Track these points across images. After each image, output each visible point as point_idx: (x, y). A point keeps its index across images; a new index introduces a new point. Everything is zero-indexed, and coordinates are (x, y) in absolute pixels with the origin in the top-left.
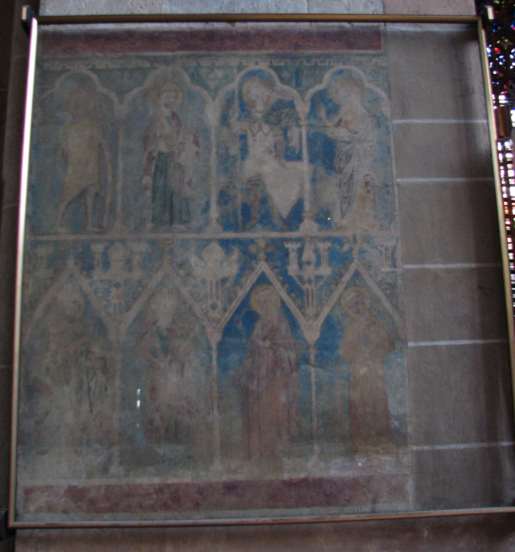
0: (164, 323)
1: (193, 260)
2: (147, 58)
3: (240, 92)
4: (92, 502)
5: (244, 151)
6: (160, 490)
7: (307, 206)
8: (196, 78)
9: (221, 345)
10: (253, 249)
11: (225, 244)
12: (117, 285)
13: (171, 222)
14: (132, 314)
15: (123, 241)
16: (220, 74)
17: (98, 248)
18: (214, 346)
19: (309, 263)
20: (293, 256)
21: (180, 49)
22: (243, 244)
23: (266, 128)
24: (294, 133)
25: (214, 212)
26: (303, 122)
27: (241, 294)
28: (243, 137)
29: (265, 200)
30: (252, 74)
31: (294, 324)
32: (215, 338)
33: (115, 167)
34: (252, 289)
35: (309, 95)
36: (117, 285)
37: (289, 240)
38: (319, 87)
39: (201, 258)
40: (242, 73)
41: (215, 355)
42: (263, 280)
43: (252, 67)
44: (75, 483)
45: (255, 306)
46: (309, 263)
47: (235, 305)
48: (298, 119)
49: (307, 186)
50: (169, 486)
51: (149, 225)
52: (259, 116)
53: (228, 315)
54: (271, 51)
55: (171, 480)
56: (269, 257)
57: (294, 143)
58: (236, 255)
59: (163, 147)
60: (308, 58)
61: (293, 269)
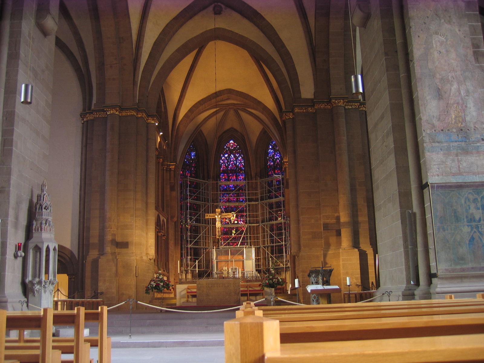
0: (458, 240)
1: (463, 229)
2: (450, 190)
3: (468, 197)
4: (450, 271)
5: (469, 208)
6: (461, 269)
7: (482, 218)
8: (459, 194)
9: (469, 243)
10: (473, 226)
11: (468, 226)
12: (450, 233)
13: (458, 222)
14: (453, 238)
15: (450, 225)
16: (464, 193)
17: (445, 227)
18: (468, 244)
19: (483, 229)
20: (480, 228)
21: (455, 188)
22: (471, 225)
23: (473, 204)
24: (478, 204)
25: (465, 220)
26: (480, 202)
27: (471, 234)
28: (469, 206)
29: (474, 217)
30: (469, 193)
31: (481, 240)
32: (467, 242)
33: (447, 211)
34: (473, 233)
35: (480, 197)
36: (450, 233)
37: (479, 224)
38: (482, 195)
39: (464, 228)
40: (468, 193)
41: (468, 245)
42: (475, 232)
43: (469, 192)
44: (446, 268)
45: (474, 236)
46: (483, 229)
47: (470, 237)
48: (479, 202)
49: (481, 214)
50: (462, 268)
51: (454, 222)
52: (471, 201)
53: (469, 238)
54: (473, 188)
55: (462, 267)
56: (476, 228)
57: (478, 206)
58: (470, 227)
59: (455, 208)
60: (480, 189)
61: (480, 230)
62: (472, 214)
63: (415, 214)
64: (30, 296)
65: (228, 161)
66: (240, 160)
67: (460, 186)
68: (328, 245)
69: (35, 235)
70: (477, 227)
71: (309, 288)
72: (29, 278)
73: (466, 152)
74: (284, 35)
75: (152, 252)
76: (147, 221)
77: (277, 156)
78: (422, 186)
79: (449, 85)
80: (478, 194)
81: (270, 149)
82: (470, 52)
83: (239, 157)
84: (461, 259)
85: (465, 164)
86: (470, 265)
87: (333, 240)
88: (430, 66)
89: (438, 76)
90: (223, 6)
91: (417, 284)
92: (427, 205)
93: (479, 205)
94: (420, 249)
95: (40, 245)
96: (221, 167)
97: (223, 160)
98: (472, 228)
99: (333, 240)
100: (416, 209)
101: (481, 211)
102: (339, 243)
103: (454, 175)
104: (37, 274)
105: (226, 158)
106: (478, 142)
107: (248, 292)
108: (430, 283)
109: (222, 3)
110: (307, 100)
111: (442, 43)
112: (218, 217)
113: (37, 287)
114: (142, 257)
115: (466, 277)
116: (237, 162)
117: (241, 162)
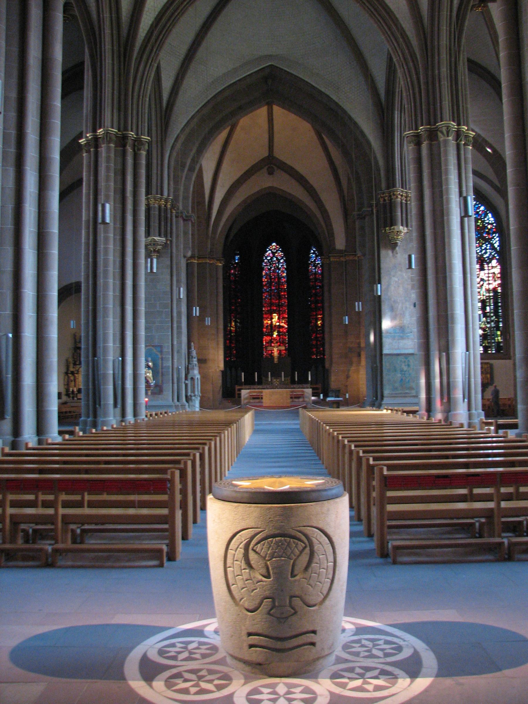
62: (403, 368)
63: (377, 366)
64: (190, 402)
65: (270, 264)
66: (281, 263)
67: (398, 355)
68: (351, 363)
69: (191, 372)
70: (404, 374)
71: (329, 399)
72: (189, 394)
73: (402, 338)
74: (324, 196)
75: (222, 366)
76: (218, 341)
77: (318, 261)
78: (381, 354)
79: (397, 305)
80: (406, 358)
81: (312, 253)
82: (410, 287)
83: (281, 259)
84: (396, 389)
85: (401, 345)
86: (400, 392)
87: (355, 359)
88: (389, 294)
89: (393, 300)
90: (275, 167)
91: (377, 399)
92: (384, 363)
93: (406, 364)
94: (379, 383)
95: (194, 377)
96: (263, 269)
97: (265, 263)
98: (402, 375)
99: (355, 359)
100: (378, 365)
101: (407, 367)
102: (359, 362)
103: (396, 349)
104: (193, 391)
105: (268, 260)
106: (409, 333)
107: (293, 396)
108: (382, 399)
109: (275, 165)
110: (340, 251)
111: (396, 282)
112: (276, 349)
113: (193, 398)
114: (216, 370)
115: (397, 397)
116: (279, 265)
117: (283, 265)
